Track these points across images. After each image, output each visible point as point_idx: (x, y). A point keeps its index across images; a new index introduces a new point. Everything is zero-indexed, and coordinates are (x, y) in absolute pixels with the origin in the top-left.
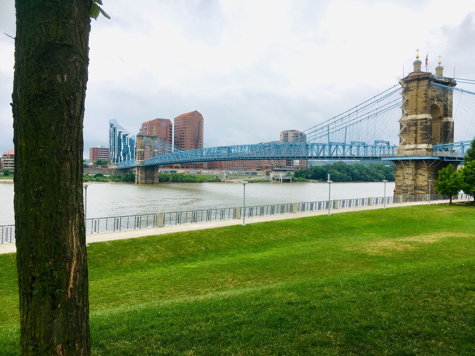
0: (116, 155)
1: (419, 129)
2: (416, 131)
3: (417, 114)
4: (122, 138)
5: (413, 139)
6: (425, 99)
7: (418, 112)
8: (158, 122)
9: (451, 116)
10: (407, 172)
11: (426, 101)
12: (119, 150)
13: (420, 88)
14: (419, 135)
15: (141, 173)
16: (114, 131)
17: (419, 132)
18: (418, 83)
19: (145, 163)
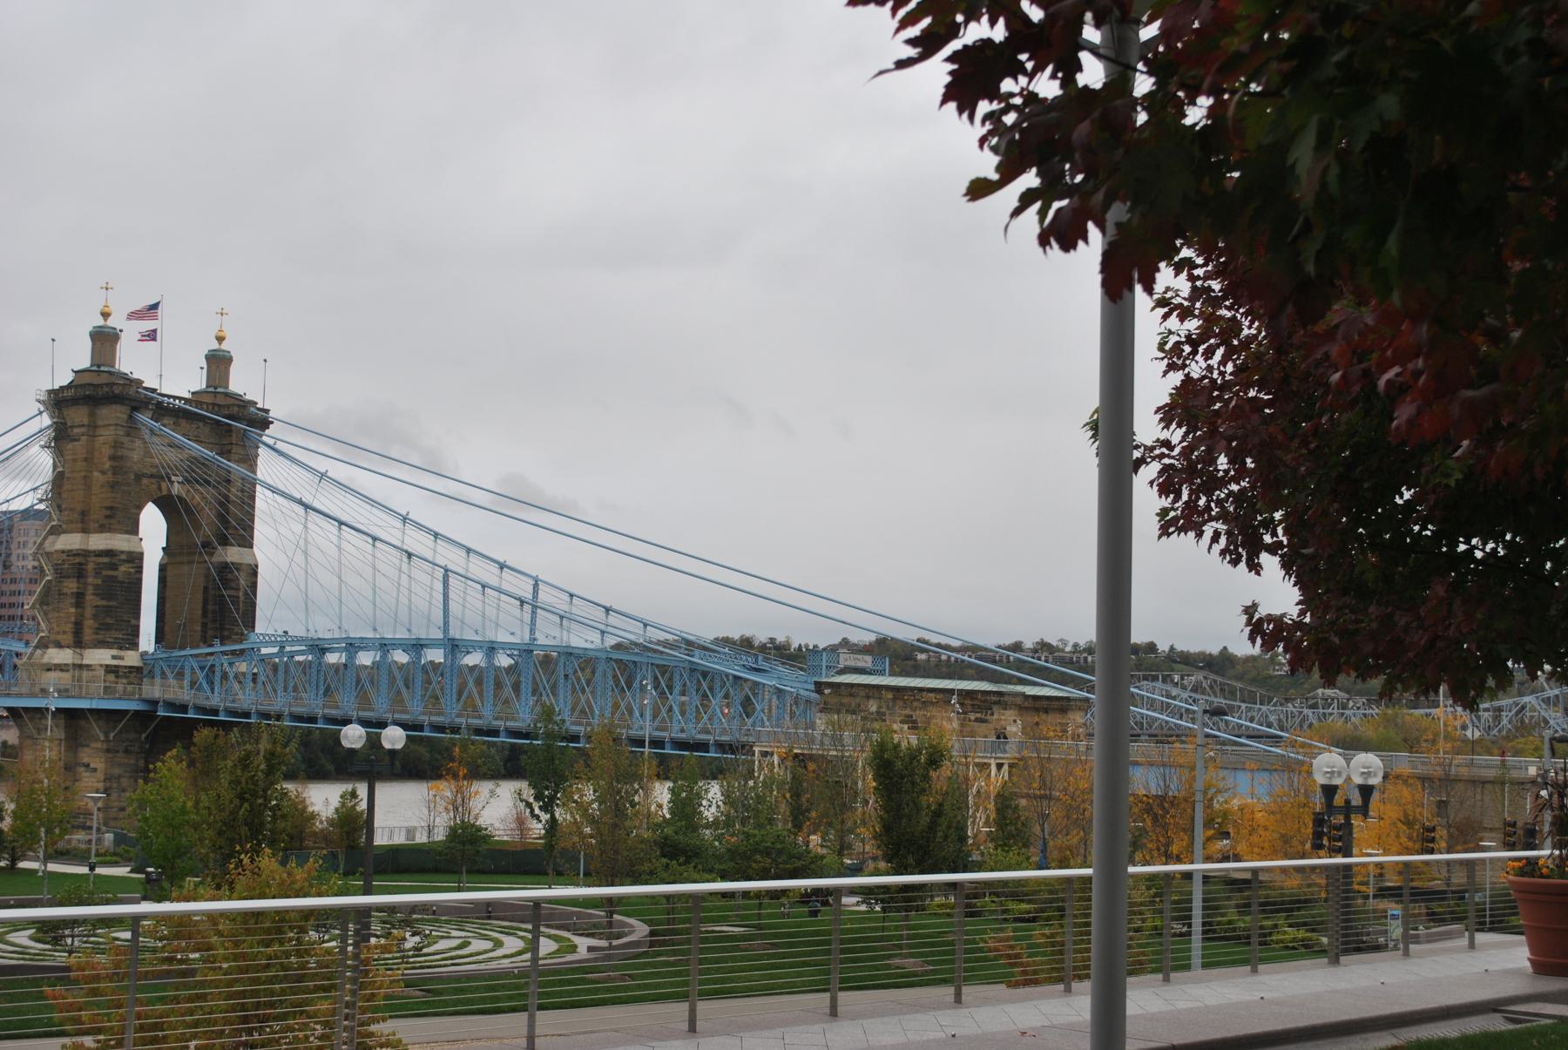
1: (90, 590)
2: (79, 598)
3: (85, 531)
5: (69, 627)
6: (109, 477)
7: (93, 526)
9: (247, 542)
11: (113, 486)
13: (101, 431)
14: (89, 612)
17: (91, 599)
18: (92, 415)
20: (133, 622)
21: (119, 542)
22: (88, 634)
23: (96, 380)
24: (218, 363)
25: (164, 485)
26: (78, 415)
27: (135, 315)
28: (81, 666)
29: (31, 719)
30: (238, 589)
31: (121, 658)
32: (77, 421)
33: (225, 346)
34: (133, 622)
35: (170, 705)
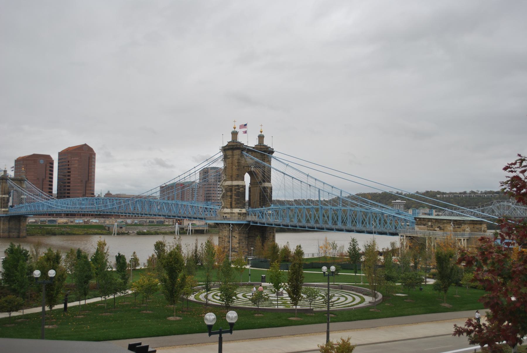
1: (233, 195)
2: (231, 196)
3: (232, 180)
5: (229, 204)
6: (237, 167)
8: (35, 158)
9: (269, 181)
10: (224, 234)
11: (238, 169)
14: (233, 200)
15: (3, 224)
17: (234, 197)
18: (232, 152)
21: (240, 183)
22: (233, 205)
23: (233, 144)
24: (261, 137)
26: (229, 153)
33: (262, 134)
35: (254, 222)
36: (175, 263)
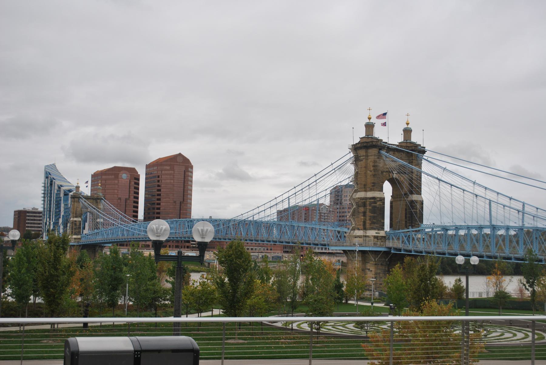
0: (52, 223)
2: (364, 214)
3: (366, 191)
4: (62, 195)
5: (362, 223)
7: (368, 189)
8: (115, 171)
9: (419, 193)
11: (374, 176)
12: (58, 214)
13: (369, 157)
14: (368, 218)
16: (51, 184)
17: (368, 213)
18: (366, 152)
19: (81, 241)
20: (382, 221)
21: (376, 194)
22: (368, 225)
24: (407, 132)
25: (391, 174)
26: (362, 152)
27: (378, 117)
28: (366, 236)
29: (351, 254)
30: (417, 209)
31: (379, 233)
32: (362, 154)
33: (409, 126)
34: (382, 221)
35: (396, 249)
36: (236, 258)
